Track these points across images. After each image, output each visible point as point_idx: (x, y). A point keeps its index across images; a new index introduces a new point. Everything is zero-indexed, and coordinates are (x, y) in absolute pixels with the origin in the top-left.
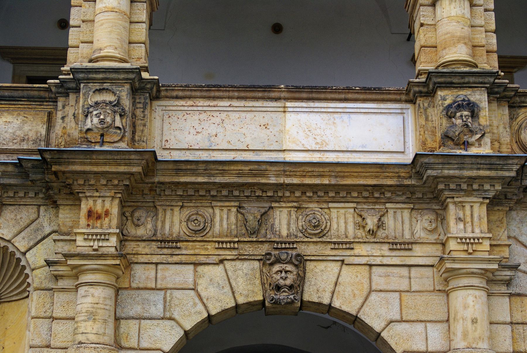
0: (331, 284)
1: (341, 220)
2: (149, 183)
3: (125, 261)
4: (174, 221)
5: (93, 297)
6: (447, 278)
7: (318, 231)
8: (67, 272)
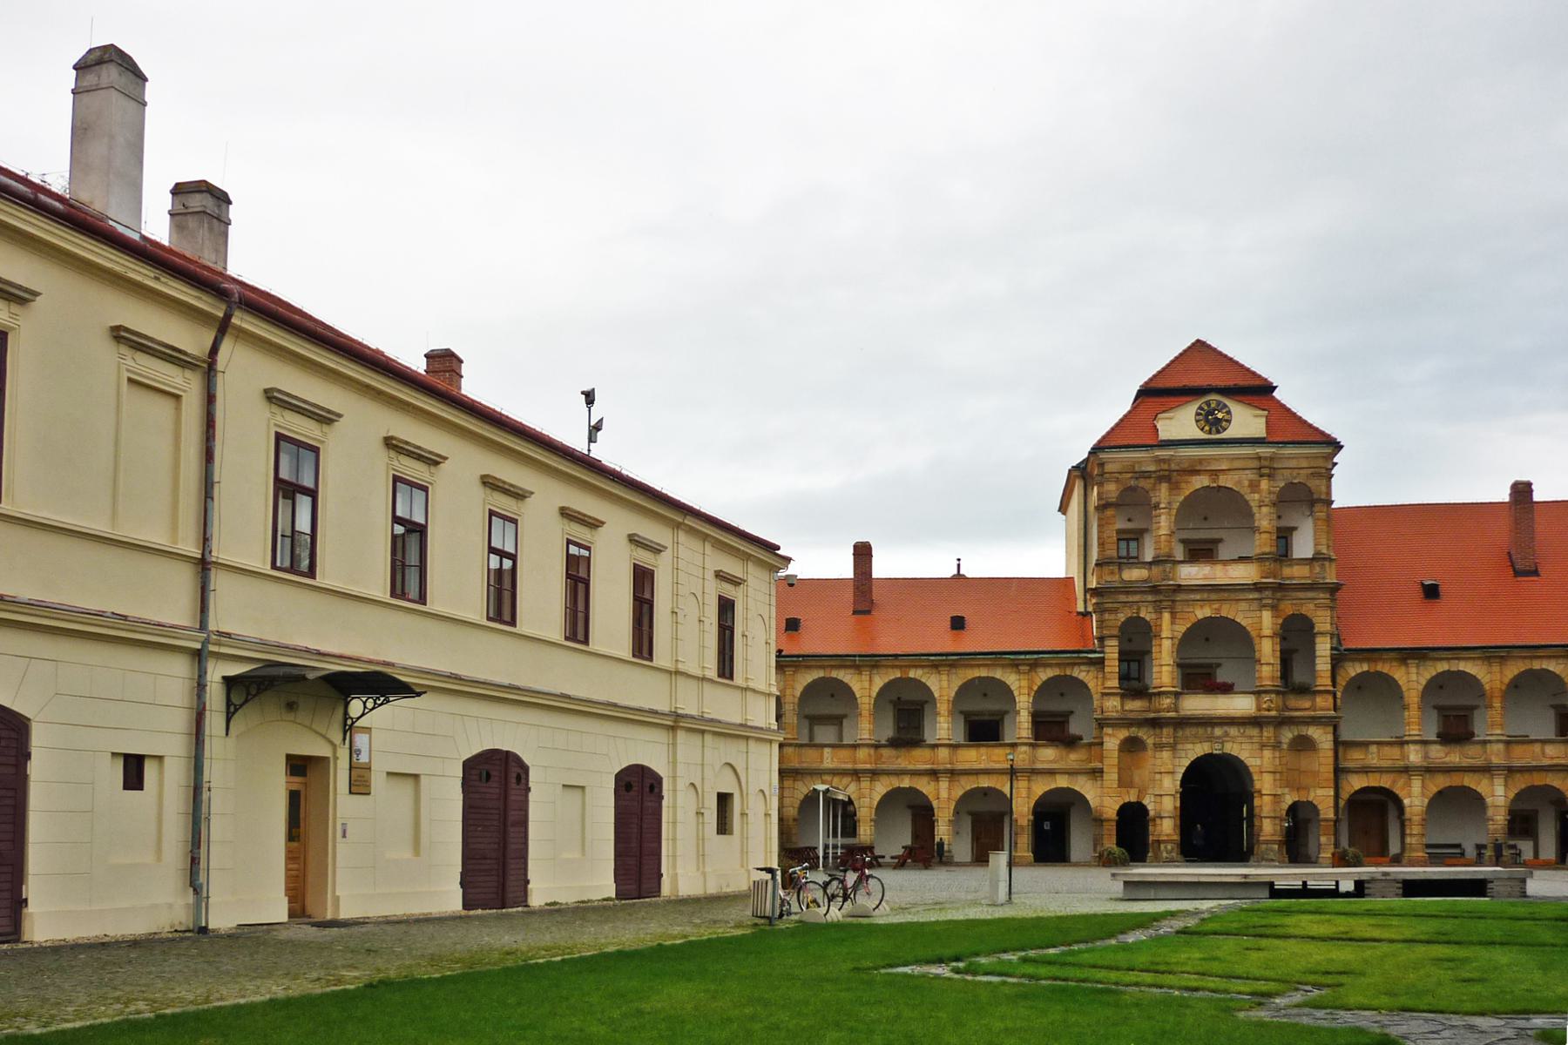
0: (1232, 749)
1: (1233, 731)
2: (1183, 722)
3: (1176, 743)
4: (1189, 731)
5: (1166, 755)
6: (1263, 746)
7: (1226, 734)
8: (1159, 747)
